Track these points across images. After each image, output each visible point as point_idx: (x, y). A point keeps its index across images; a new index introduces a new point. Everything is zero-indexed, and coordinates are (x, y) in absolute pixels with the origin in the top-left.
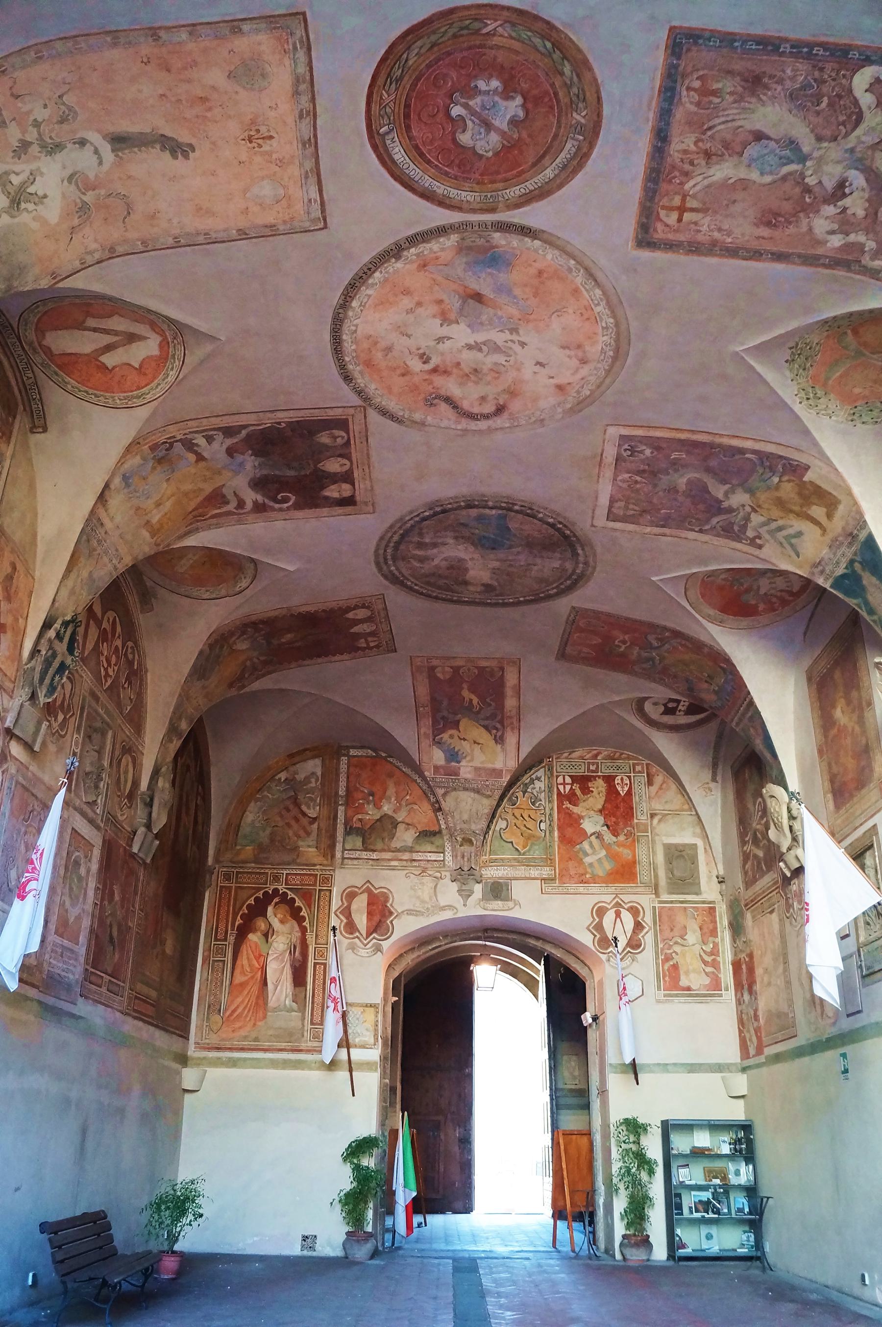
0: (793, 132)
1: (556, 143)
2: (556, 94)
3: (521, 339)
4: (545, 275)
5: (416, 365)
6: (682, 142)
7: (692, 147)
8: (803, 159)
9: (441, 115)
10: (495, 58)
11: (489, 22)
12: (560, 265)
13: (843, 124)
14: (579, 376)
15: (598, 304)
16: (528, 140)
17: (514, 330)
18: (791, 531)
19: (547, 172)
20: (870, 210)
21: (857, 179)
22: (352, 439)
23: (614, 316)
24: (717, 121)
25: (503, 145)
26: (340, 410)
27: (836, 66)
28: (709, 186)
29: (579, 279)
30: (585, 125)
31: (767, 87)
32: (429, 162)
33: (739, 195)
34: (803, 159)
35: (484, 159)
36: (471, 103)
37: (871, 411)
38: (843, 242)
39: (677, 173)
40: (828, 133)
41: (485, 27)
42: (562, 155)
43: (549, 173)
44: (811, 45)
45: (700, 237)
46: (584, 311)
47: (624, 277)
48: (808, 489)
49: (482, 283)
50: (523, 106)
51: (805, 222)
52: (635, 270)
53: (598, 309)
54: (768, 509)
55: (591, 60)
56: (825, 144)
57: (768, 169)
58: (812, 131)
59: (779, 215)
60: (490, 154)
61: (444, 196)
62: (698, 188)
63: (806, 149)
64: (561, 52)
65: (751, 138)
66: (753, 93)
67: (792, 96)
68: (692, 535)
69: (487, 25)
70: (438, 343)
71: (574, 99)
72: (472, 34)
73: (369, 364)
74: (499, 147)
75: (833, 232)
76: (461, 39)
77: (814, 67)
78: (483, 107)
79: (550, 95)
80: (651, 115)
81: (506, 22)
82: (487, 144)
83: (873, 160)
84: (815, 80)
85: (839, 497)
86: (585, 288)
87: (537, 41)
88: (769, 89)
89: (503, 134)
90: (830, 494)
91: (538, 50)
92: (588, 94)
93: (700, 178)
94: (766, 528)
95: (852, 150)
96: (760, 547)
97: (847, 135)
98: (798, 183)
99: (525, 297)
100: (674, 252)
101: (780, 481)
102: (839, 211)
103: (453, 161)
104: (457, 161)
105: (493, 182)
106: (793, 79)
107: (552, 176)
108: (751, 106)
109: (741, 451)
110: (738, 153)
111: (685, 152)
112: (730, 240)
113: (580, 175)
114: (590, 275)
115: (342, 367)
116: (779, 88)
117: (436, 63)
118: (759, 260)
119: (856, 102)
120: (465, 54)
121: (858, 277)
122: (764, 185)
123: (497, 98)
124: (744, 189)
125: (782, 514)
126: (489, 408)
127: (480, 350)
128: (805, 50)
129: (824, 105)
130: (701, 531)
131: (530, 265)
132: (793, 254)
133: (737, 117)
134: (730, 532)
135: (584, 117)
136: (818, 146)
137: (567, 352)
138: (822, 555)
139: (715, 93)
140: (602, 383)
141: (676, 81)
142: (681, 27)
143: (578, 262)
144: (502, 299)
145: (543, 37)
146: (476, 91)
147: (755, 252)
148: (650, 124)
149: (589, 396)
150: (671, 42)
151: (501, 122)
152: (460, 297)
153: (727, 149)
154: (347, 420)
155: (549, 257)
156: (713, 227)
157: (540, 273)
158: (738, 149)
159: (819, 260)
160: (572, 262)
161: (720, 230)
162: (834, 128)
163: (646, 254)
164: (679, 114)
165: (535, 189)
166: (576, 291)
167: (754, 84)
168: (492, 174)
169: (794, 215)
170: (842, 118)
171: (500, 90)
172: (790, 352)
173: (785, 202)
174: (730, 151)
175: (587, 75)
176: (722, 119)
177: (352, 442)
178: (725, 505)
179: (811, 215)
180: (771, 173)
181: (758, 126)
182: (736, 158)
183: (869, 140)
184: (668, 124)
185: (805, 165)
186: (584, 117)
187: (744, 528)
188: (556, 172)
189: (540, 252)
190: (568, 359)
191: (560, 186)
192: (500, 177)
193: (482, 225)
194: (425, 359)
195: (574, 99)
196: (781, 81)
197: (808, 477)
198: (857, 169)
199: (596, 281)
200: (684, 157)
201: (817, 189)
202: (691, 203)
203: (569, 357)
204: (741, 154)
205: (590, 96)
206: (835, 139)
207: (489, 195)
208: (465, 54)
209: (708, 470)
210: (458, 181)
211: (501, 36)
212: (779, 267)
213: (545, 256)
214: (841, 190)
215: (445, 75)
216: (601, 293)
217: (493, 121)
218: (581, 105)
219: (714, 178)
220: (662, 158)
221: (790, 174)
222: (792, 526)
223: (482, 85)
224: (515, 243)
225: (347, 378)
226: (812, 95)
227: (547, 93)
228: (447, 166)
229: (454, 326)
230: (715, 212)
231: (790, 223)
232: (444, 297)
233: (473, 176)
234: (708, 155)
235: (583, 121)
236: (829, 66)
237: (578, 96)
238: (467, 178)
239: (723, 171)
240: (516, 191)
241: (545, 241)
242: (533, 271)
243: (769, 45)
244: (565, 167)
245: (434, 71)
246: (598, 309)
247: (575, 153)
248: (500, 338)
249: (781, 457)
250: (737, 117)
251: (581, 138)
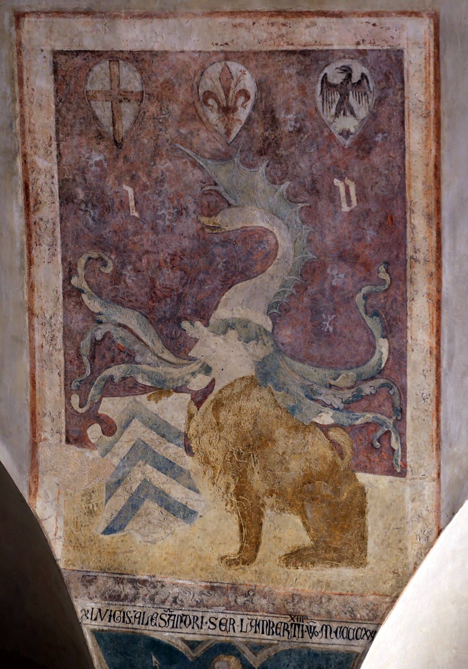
18: (178, 492)
48: (337, 491)
54: (219, 426)
68: (50, 275)
85: (369, 559)
90: (364, 538)
94: (150, 436)
96: (76, 438)
101: (325, 429)
109: (394, 326)
125: (217, 455)
130: (71, 293)
134: (94, 364)
138: (168, 580)
178: (194, 329)
187: (111, 388)
197: (375, 483)
209: (310, 271)
222: (193, 488)
249: (400, 412)
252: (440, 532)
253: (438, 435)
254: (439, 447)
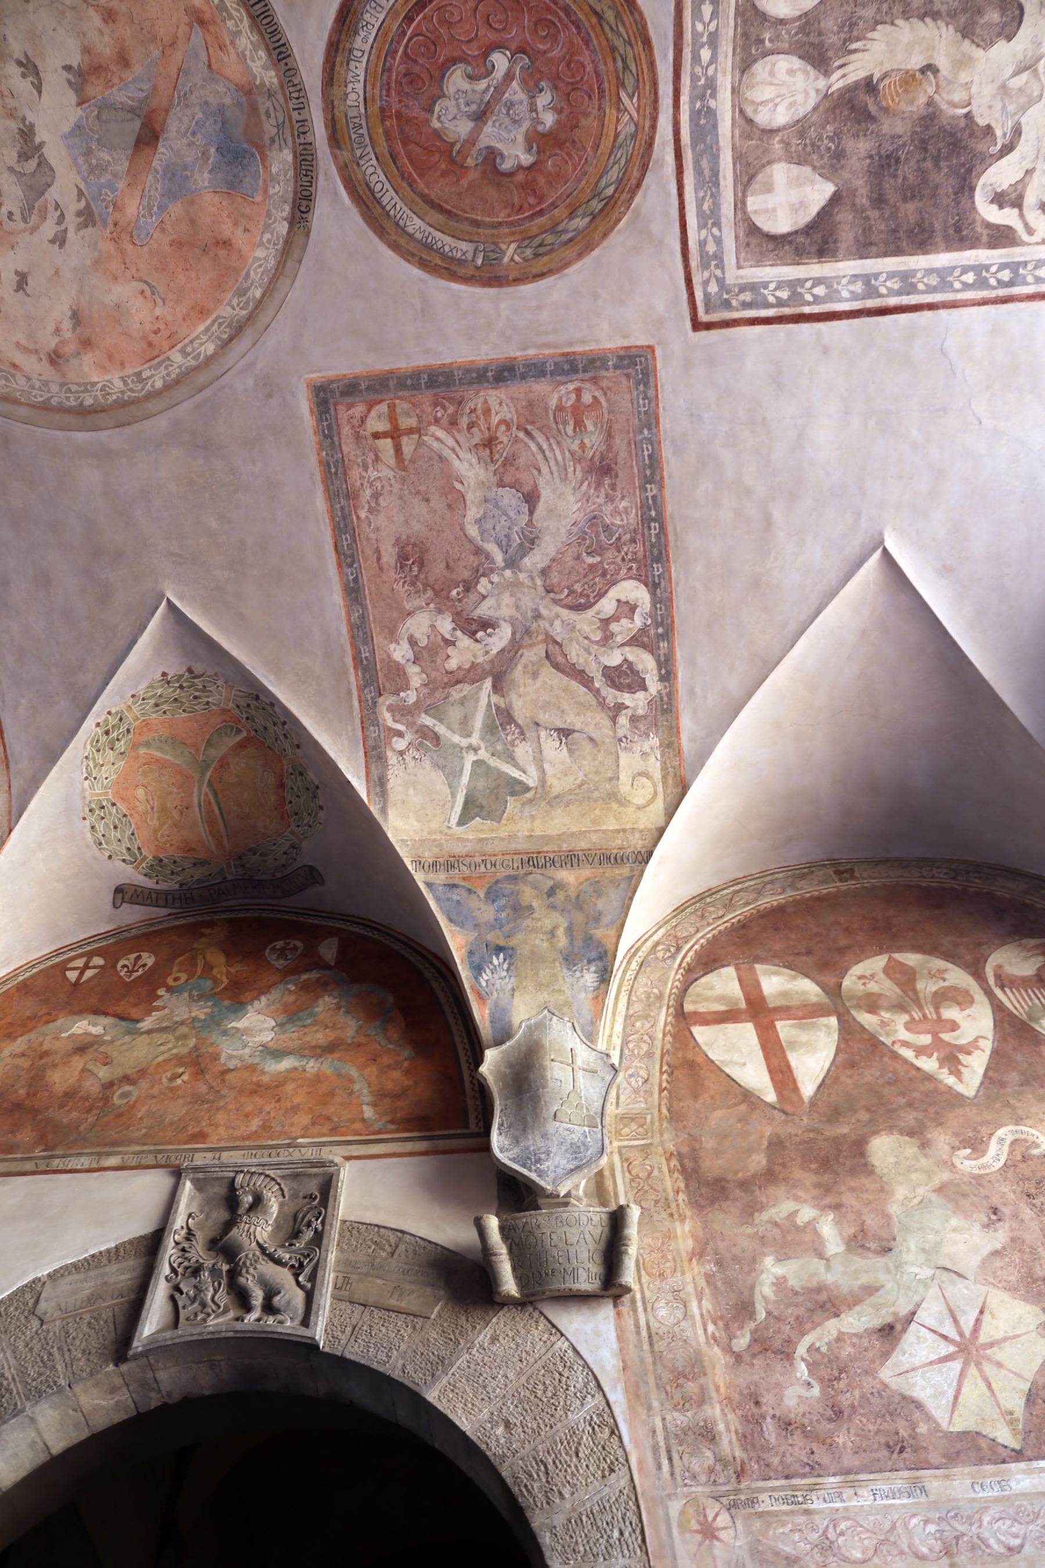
0: (547, 538)
1: (466, 227)
2: (541, 213)
3: (71, 235)
4: (222, 253)
6: (500, 403)
7: (495, 420)
8: (512, 563)
9: (492, 36)
10: (586, 115)
11: (635, 100)
12: (248, 274)
13: (572, 592)
14: (19, 358)
15: (185, 354)
16: (465, 182)
17: (87, 218)
19: (417, 221)
20: (462, 673)
21: (499, 639)
23: (167, 387)
24: (541, 439)
25: (453, 144)
27: (641, 554)
28: (441, 458)
29: (229, 310)
30: (499, 264)
31: (599, 485)
32: (409, 19)
33: (438, 502)
34: (512, 563)
35: (427, 116)
36: (515, 84)
37: (115, 827)
38: (403, 662)
39: (451, 410)
40: (555, 578)
41: (628, 94)
42: (447, 239)
43: (415, 225)
44: (660, 519)
45: (355, 473)
46: (164, 333)
47: (250, 382)
49: (177, 143)
50: (520, 167)
51: (420, 602)
52: (269, 396)
53: (177, 357)
55: (596, 252)
56: (539, 582)
57: (489, 526)
58: (553, 560)
59: (421, 565)
60: (436, 124)
61: (351, 51)
62: (436, 445)
63: (527, 562)
64: (601, 210)
65: (527, 489)
66: (589, 471)
67: (593, 520)
69: (631, 97)
71: (537, 241)
72: (618, 78)
74: (450, 138)
75: (412, 642)
76: (609, 60)
77: (635, 531)
78: (510, 105)
79: (539, 204)
80: (532, 352)
81: (636, 125)
82: (451, 120)
83: (532, 645)
84: (619, 539)
86: (212, 324)
87: (614, 174)
88: (596, 489)
89: (472, 140)
91: (601, 177)
92: (545, 259)
93: (450, 442)
95: (538, 616)
97: (555, 602)
98: (477, 571)
99: (168, 227)
100: (320, 443)
102: (448, 636)
103: (415, 61)
104: (417, 69)
105: (387, 133)
106: (616, 512)
107: (410, 230)
108: (570, 475)
110: (501, 480)
111: (487, 411)
112: (363, 514)
113: (416, 272)
114: (238, 329)
116: (601, 500)
117: (573, 23)
118: (339, 565)
119: (601, 595)
120: (589, 68)
121: (356, 704)
122: (462, 529)
123: (526, 124)
124: (449, 506)
127: (24, 156)
128: (653, 513)
129: (590, 560)
131: (236, 224)
132: (364, 607)
133: (552, 463)
135: (512, 259)
136: (535, 574)
137: (67, 325)
139: (579, 424)
140: (16, 402)
141: (585, 371)
142: (654, 359)
143: (260, 302)
144: (153, 183)
145: (619, 181)
146: (533, 89)
147: (352, 556)
148: (518, 354)
150: (634, 352)
151: (491, 135)
152: (141, 101)
153: (504, 465)
155: (260, 253)
156: (378, 484)
157: (226, 244)
158: (508, 478)
159: (365, 643)
160: (258, 293)
161: (376, 496)
162: (563, 584)
163: (304, 406)
164: (540, 387)
165: (383, 208)
166: (203, 312)
167: (603, 469)
168: (402, 131)
169: (426, 585)
170: (578, 588)
171: (540, 128)
172: (182, 670)
173: (443, 565)
174: (501, 470)
175: (570, 253)
176: (545, 446)
179: (432, 606)
180: (482, 532)
181: (546, 493)
182: (494, 480)
183: (558, 630)
184: (523, 377)
185: (503, 569)
186: (512, 259)
188: (419, 236)
189: (267, 236)
190: (51, 328)
191: (395, 247)
192: (399, 147)
193: (303, 128)
195: (537, 241)
196: (610, 499)
198: (514, 634)
199: (231, 339)
200: (479, 412)
201: (473, 597)
202: (408, 445)
203: (57, 331)
204: (501, 484)
205: (538, 267)
206: (548, 592)
207: (364, 131)
208: (589, 68)
210: (380, 72)
211: (618, 120)
212: (337, 597)
213: (261, 244)
214: (476, 626)
215: (555, 38)
216: (210, 352)
217: (490, 123)
218: (529, 252)
219: (456, 463)
220: (471, 383)
221: (488, 556)
223: (544, 99)
224: (275, 190)
226: (599, 541)
227: (541, 199)
228: (405, 52)
229: (72, 97)
230: (403, 480)
231: (413, 584)
232: (137, 69)
233: (394, 98)
234: (489, 443)
235: (506, 259)
236: (639, 548)
237: (540, 245)
238: (388, 90)
239: (470, 470)
240: (376, 175)
241: (288, 242)
242: (227, 229)
243: (652, 471)
244: (429, 247)
245: (560, 20)
246: (177, 357)
247: (452, 259)
250: (552, 463)
251: (479, 262)
252: (10, 831)
253: (6, 757)
254: (8, 767)
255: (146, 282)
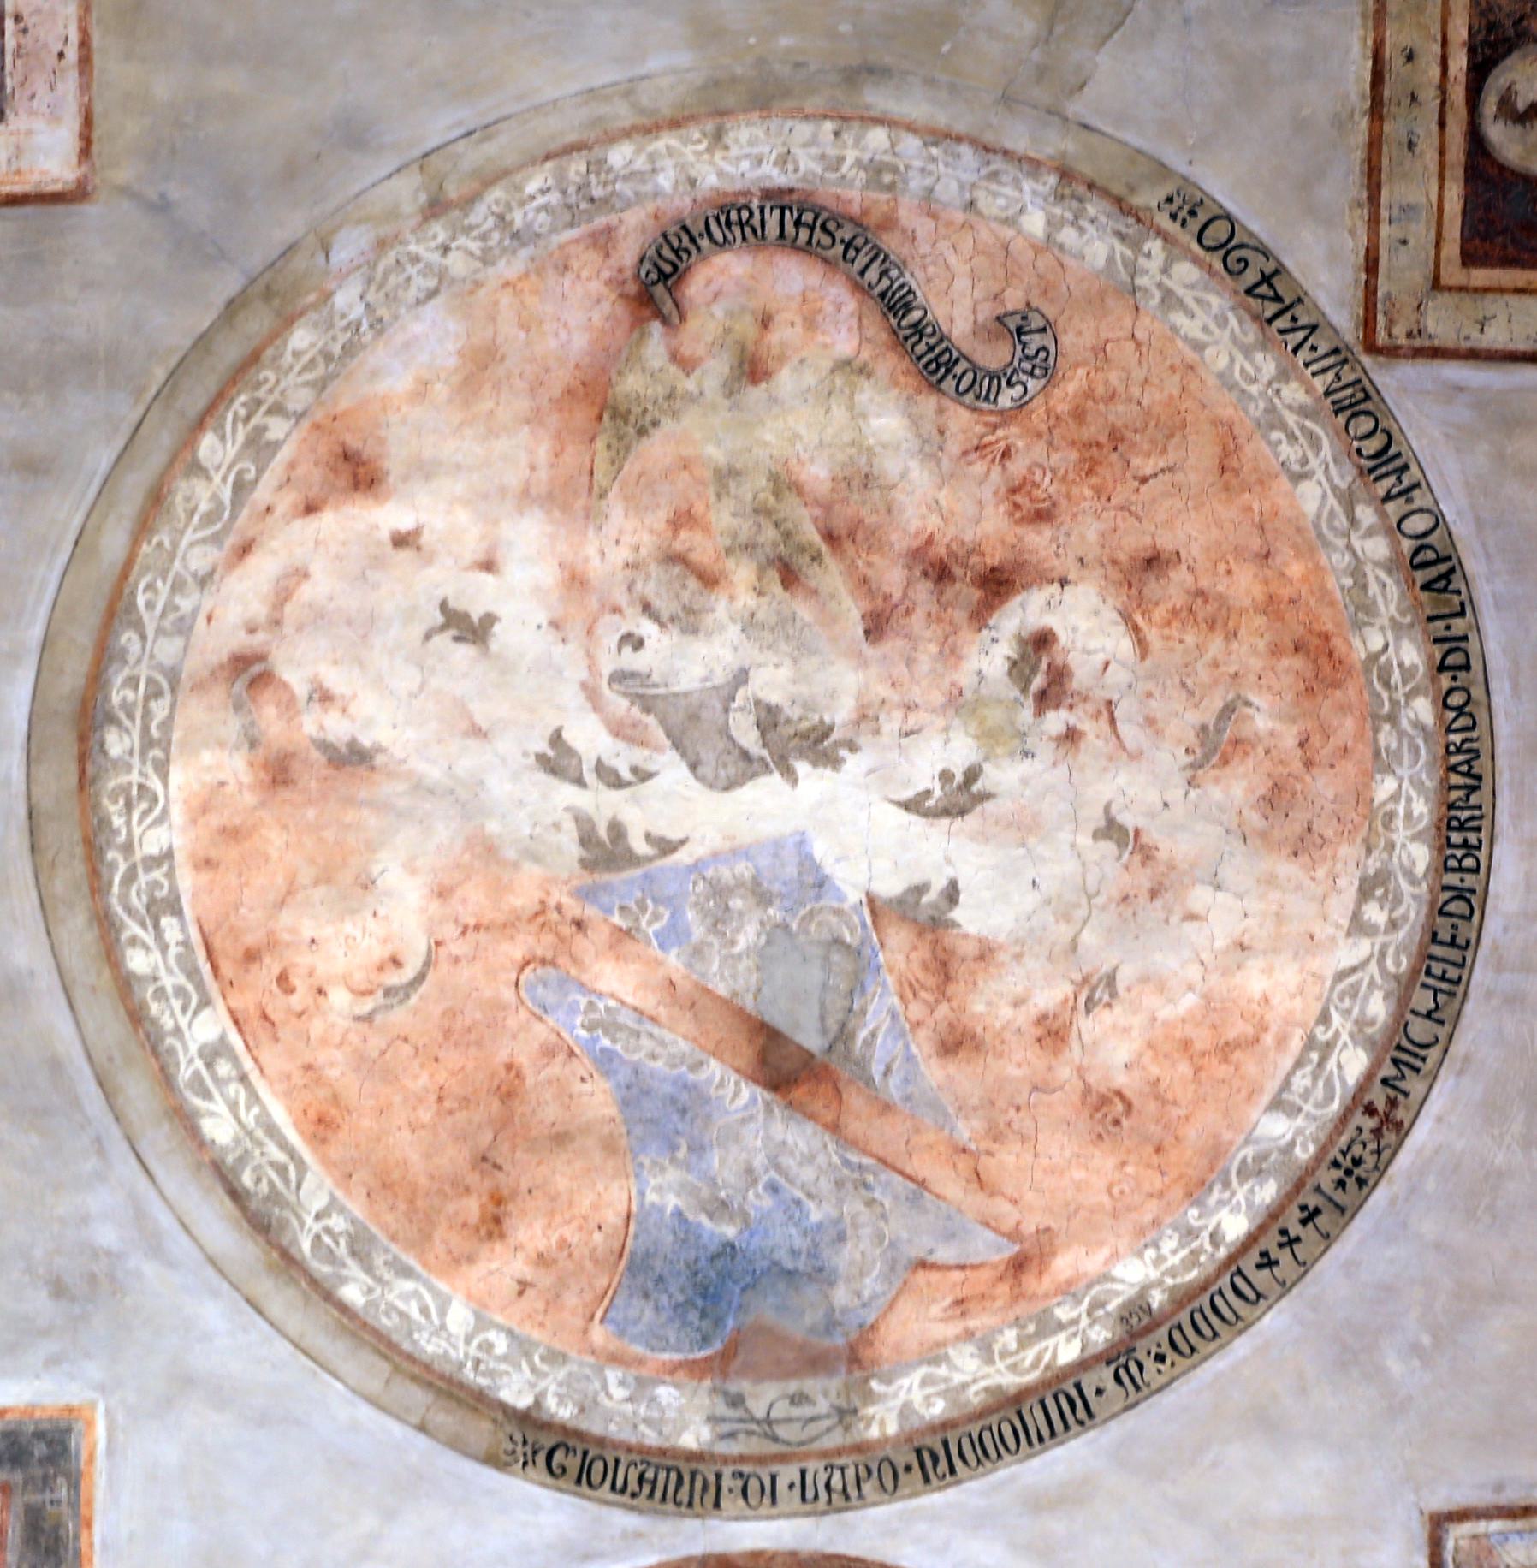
3: (566, 794)
4: (472, 1207)
5: (1085, 623)
12: (406, 1272)
14: (263, 569)
15: (214, 1053)
17: (605, 851)
22: (1458, 94)
23: (125, 984)
26: (1496, 336)
29: (319, 1203)
46: (278, 1005)
47: (107, 1236)
49: (757, 1133)
52: (59, 1290)
53: (208, 1027)
70: (972, 774)
73: (1319, 660)
86: (284, 1145)
99: (556, 1068)
114: (261, 1221)
115: (1454, 659)
126: (722, 278)
127: (769, 719)
131: (542, 1260)
137: (337, 728)
140: (143, 527)
143: (329, 1297)
144: (668, 1050)
149: (199, 426)
152: (863, 1064)
154: (1469, 259)
155: (459, 1317)
157: (494, 1225)
160: (352, 1294)
166: (322, 1126)
177: (1459, 63)
189: (501, 1345)
190: (334, 679)
193: (759, 1493)
194: (1042, 669)
199: (236, 1195)
203: (323, 696)
213: (482, 1323)
216: (209, 1127)
224: (615, 1387)
225: (1435, 573)
229: (890, 886)
232: (934, 1072)
241: (479, 1401)
242: (531, 1232)
246: (208, 1027)
248: (675, 805)
255: (421, 978)
